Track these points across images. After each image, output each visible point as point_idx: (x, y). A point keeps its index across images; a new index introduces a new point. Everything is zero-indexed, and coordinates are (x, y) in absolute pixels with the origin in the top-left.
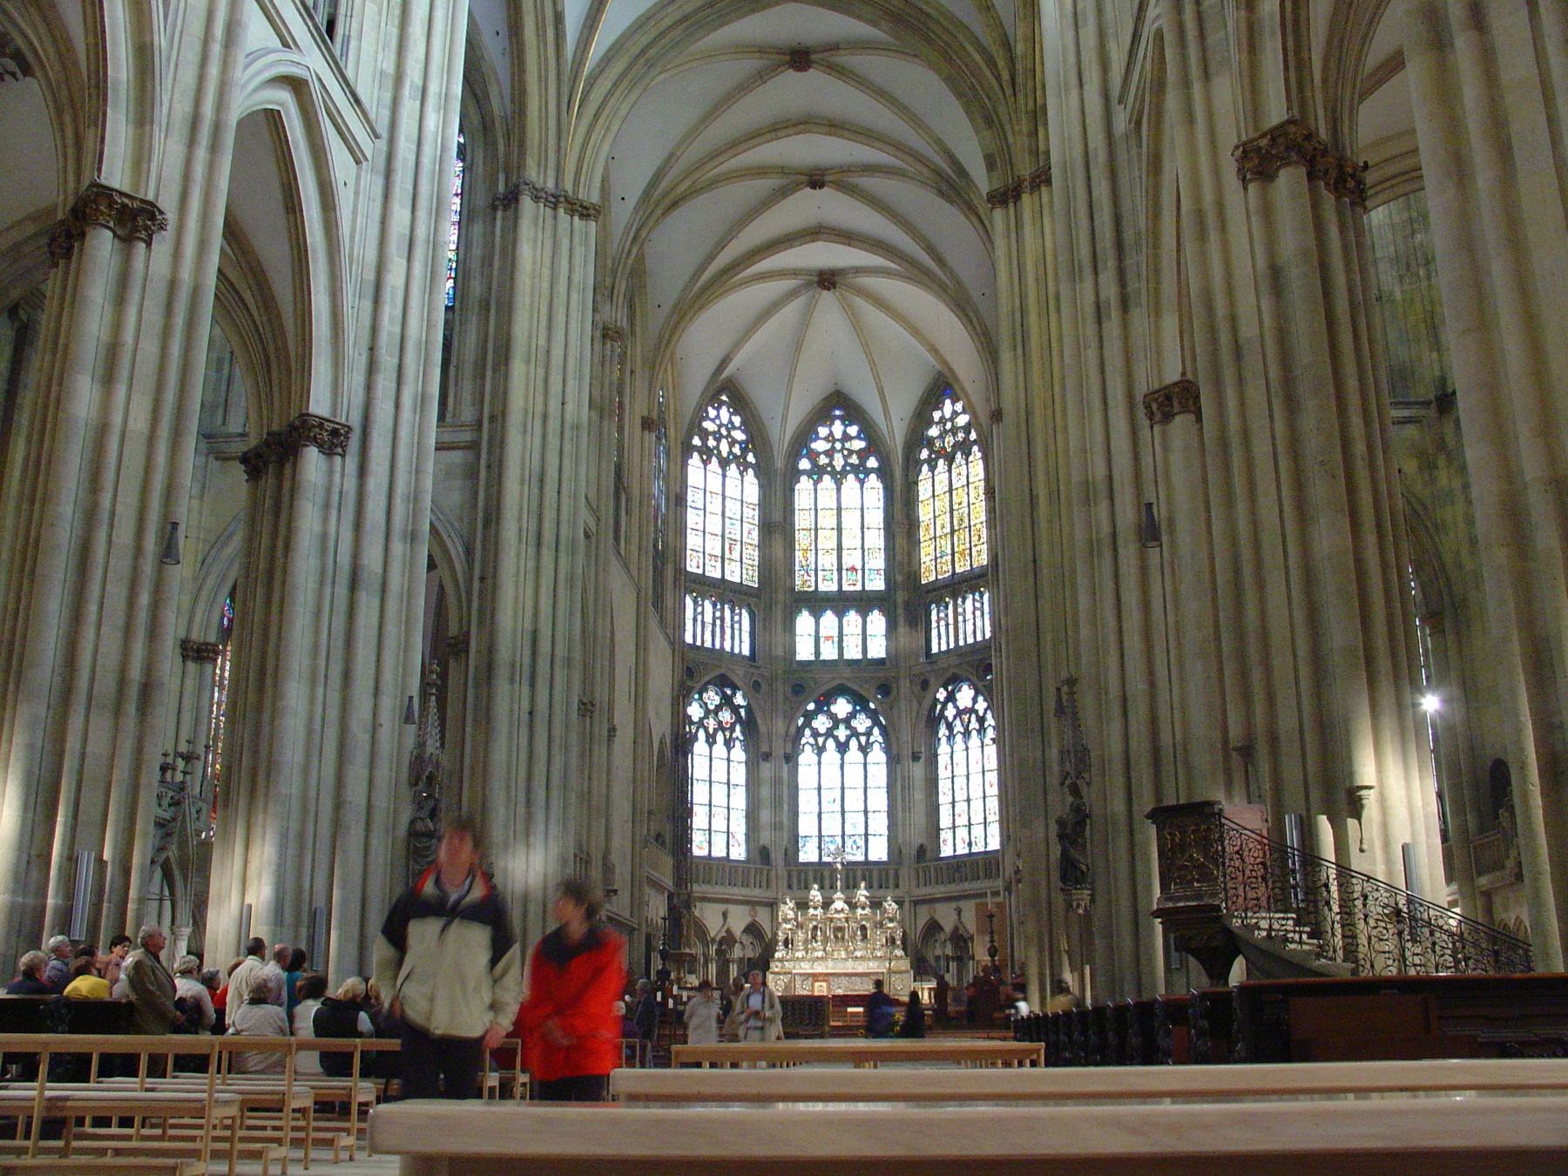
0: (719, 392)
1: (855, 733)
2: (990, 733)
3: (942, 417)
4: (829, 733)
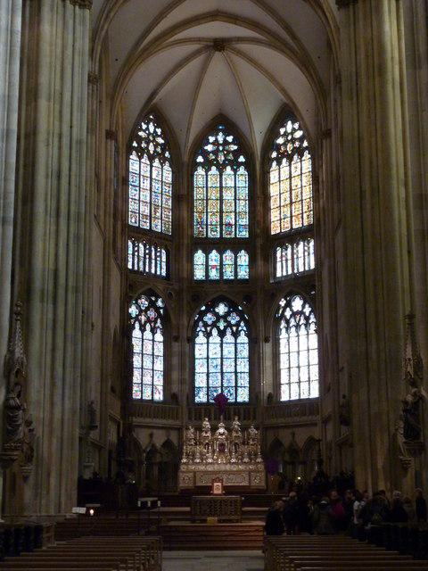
0: (149, 114)
1: (229, 325)
2: (313, 327)
3: (285, 132)
4: (214, 325)
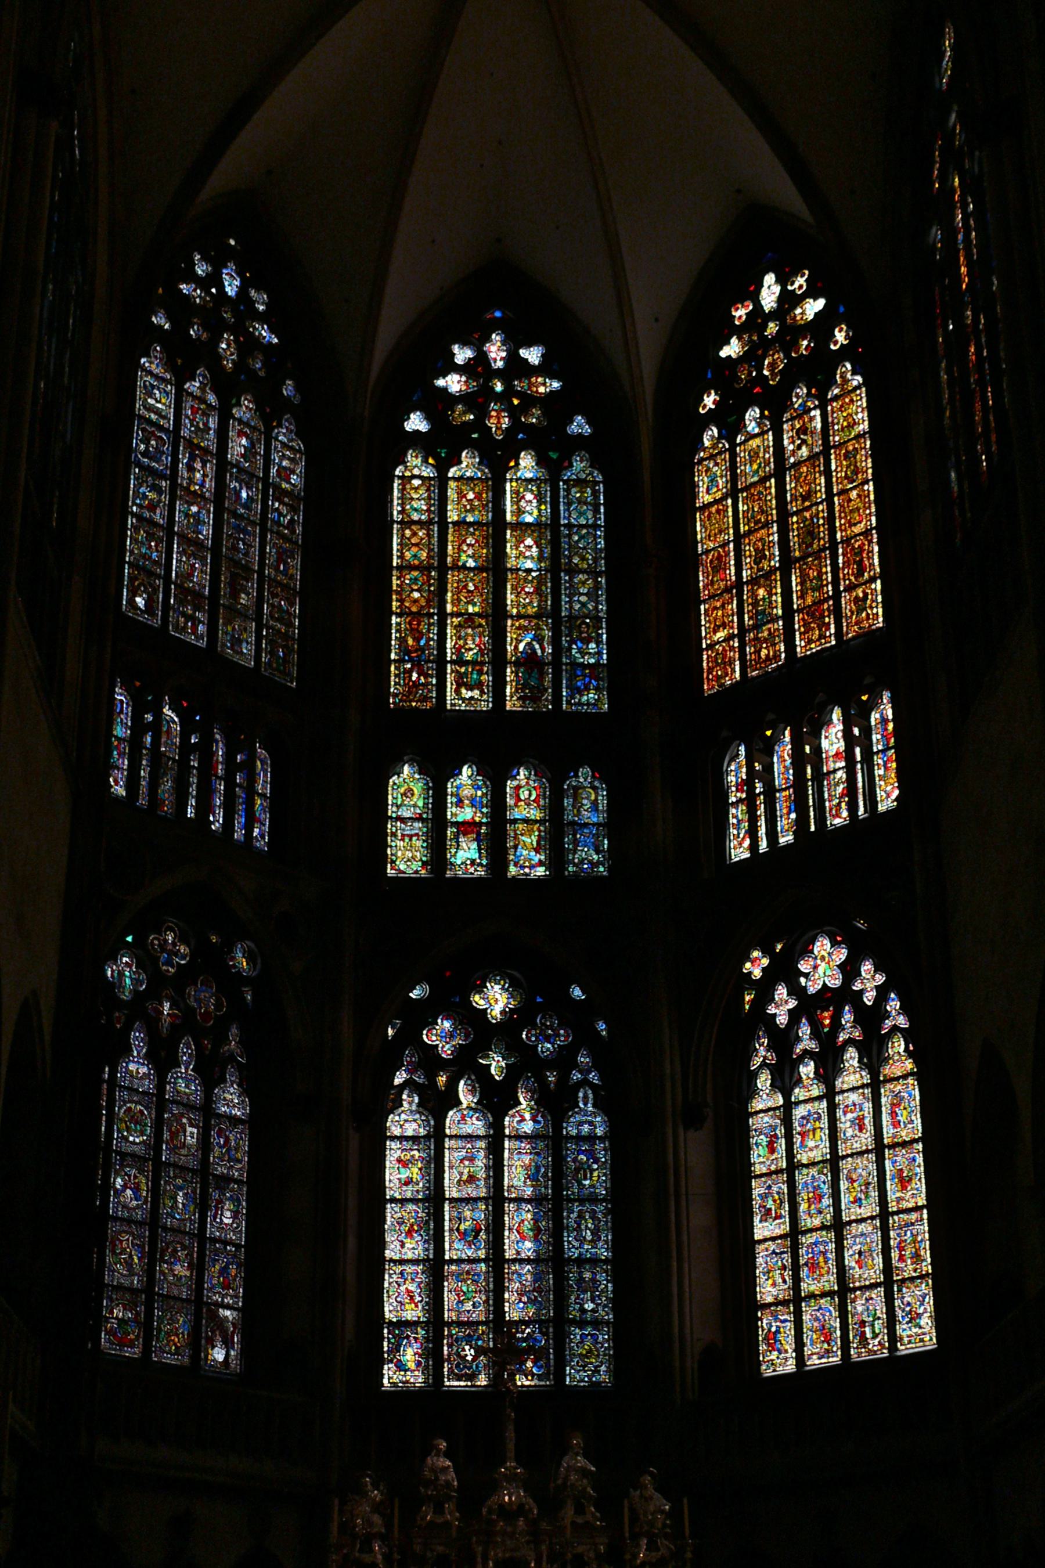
2: (898, 1046)
